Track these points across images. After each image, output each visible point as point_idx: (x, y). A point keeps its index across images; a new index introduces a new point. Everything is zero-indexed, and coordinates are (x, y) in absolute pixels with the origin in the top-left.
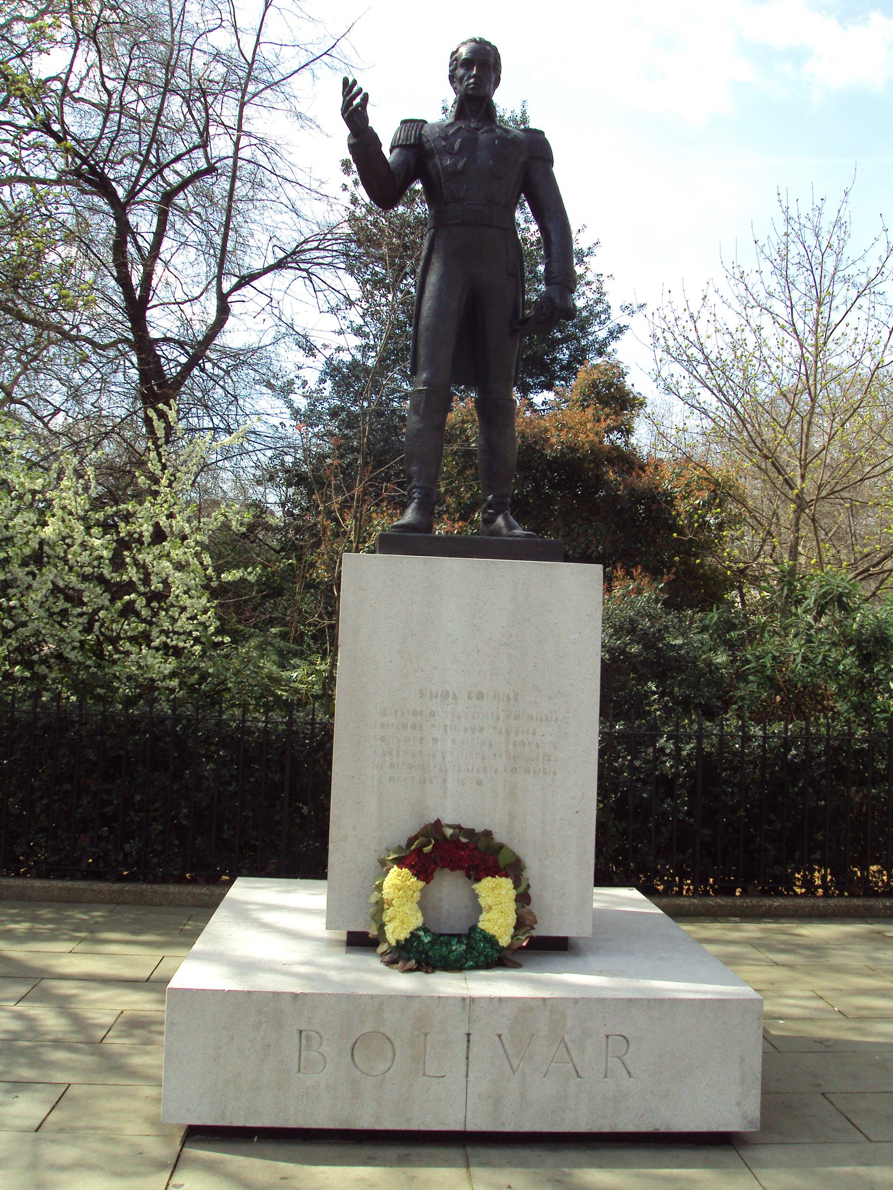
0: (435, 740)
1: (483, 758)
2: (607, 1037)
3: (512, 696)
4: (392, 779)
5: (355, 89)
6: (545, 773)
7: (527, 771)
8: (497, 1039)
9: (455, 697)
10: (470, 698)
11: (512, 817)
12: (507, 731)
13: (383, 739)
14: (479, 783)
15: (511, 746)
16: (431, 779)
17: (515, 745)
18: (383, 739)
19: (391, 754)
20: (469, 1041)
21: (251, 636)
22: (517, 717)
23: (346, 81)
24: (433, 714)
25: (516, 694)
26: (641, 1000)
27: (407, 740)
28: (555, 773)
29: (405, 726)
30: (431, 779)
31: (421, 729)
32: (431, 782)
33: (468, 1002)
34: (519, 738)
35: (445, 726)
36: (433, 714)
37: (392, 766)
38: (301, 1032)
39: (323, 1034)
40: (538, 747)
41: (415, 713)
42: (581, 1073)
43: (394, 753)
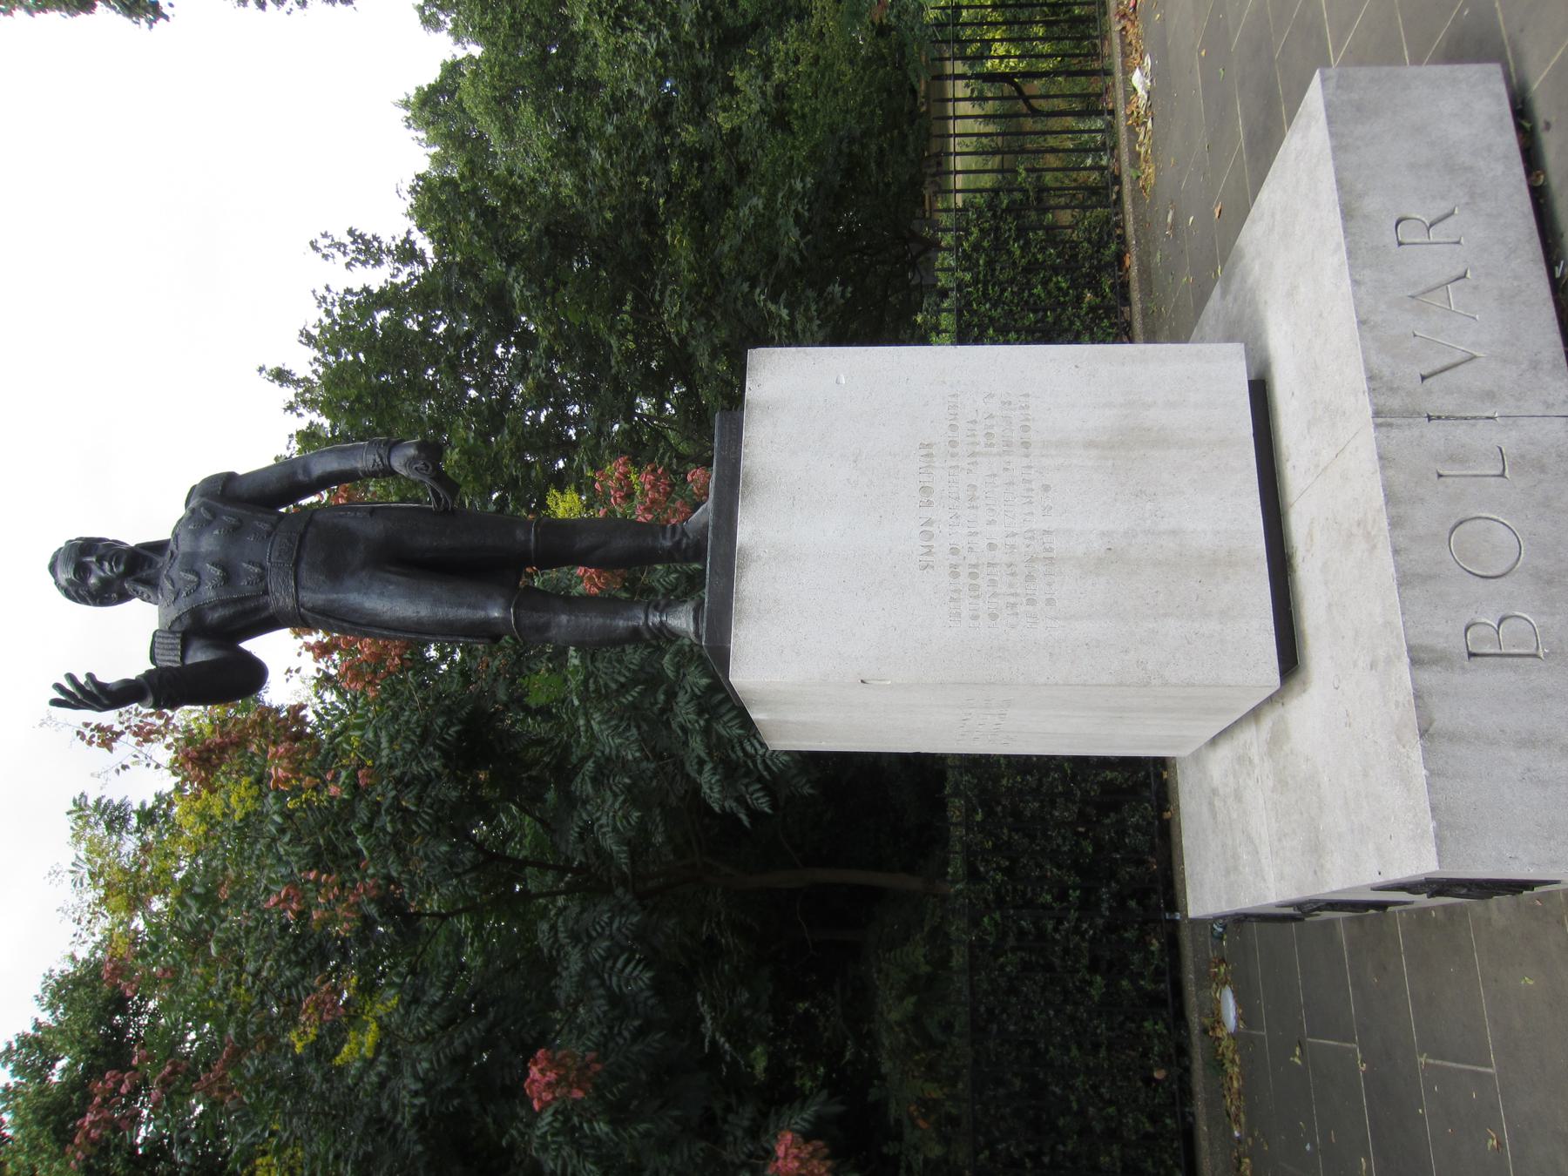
0: (991, 546)
1: (1011, 483)
2: (1400, 244)
3: (924, 452)
4: (1050, 602)
5: (68, 687)
6: (1027, 407)
7: (1025, 429)
8: (1428, 382)
9: (929, 522)
10: (930, 504)
11: (1090, 444)
12: (973, 454)
13: (993, 617)
14: (1046, 488)
15: (995, 450)
16: (1046, 550)
17: (992, 445)
18: (993, 617)
19: (1014, 605)
20: (1439, 418)
21: (718, 734)
22: (953, 443)
23: (55, 702)
24: (954, 551)
25: (923, 446)
26: (1338, 170)
27: (993, 583)
28: (1027, 395)
29: (974, 588)
30: (1046, 550)
31: (975, 566)
32: (1051, 550)
33: (1380, 420)
34: (982, 440)
35: (971, 534)
36: (954, 551)
37: (1031, 602)
38: (1471, 655)
39: (1467, 620)
40: (991, 416)
41: (955, 575)
42: (1459, 271)
43: (1012, 600)
